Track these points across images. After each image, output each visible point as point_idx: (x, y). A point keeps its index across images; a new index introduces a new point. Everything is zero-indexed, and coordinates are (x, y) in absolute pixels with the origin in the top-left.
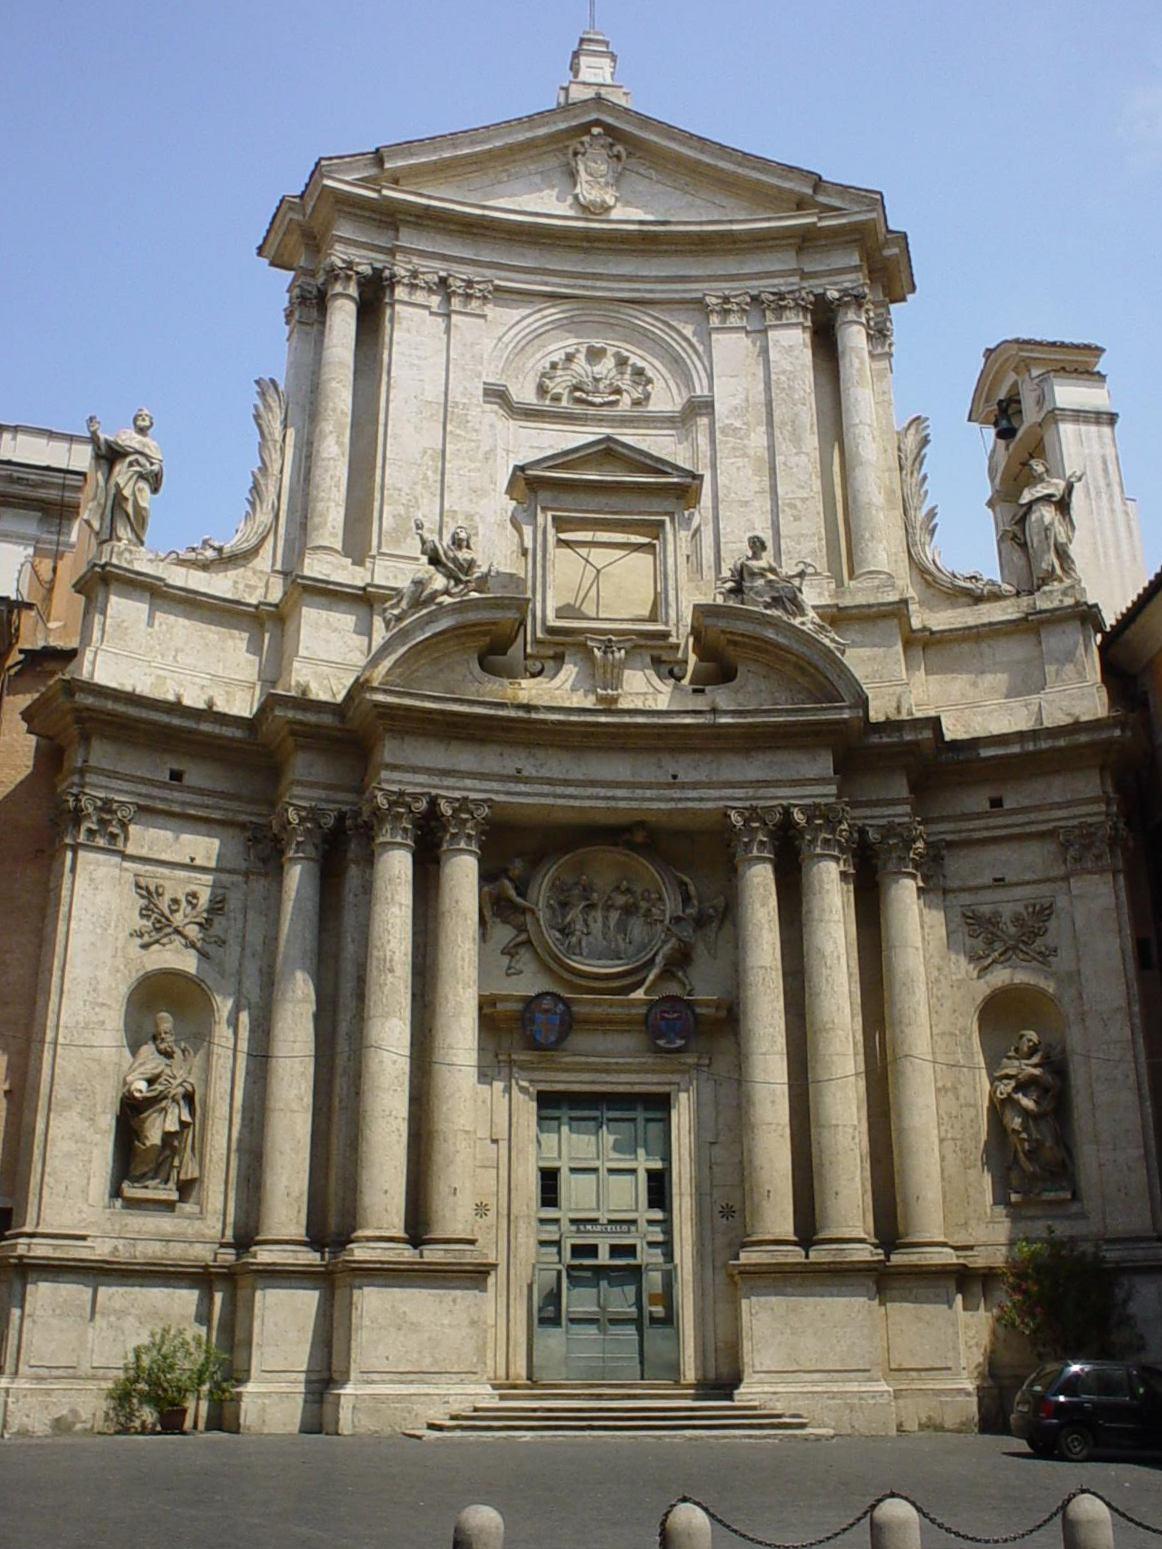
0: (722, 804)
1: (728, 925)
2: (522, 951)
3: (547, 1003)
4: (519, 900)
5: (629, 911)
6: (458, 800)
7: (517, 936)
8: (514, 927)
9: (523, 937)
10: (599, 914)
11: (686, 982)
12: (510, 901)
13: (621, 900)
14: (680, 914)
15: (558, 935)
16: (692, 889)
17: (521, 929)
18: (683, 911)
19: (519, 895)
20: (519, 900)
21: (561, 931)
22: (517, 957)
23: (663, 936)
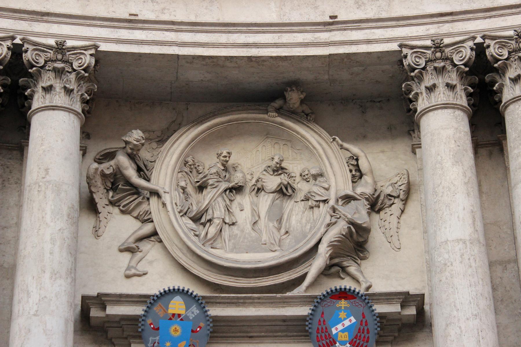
0: (394, 47)
1: (413, 206)
2: (145, 246)
3: (177, 305)
4: (142, 182)
5: (284, 192)
6: (50, 47)
7: (140, 229)
8: (136, 218)
9: (147, 228)
10: (245, 200)
11: (361, 279)
12: (128, 182)
13: (273, 182)
14: (350, 192)
15: (191, 224)
16: (363, 164)
17: (146, 219)
18: (354, 189)
19: (140, 176)
20: (142, 182)
21: (196, 219)
22: (139, 255)
23: (328, 218)
